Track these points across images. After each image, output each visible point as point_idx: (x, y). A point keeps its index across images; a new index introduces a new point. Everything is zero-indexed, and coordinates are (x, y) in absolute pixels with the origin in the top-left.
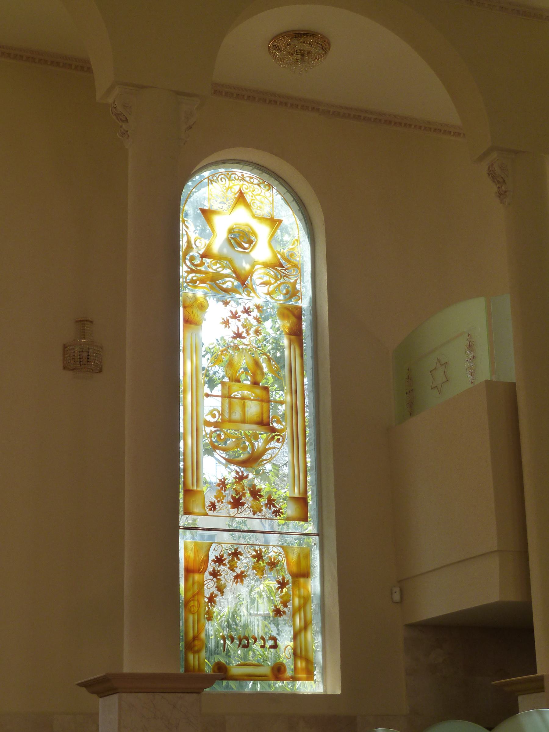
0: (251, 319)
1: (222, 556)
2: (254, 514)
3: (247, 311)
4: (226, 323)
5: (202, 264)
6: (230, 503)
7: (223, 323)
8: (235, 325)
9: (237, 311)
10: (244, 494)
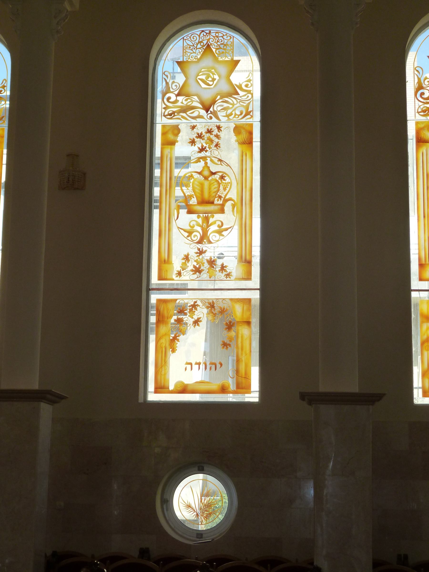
0: (212, 137)
2: (210, 278)
3: (209, 131)
6: (192, 270)
7: (190, 142)
8: (199, 143)
9: (202, 132)
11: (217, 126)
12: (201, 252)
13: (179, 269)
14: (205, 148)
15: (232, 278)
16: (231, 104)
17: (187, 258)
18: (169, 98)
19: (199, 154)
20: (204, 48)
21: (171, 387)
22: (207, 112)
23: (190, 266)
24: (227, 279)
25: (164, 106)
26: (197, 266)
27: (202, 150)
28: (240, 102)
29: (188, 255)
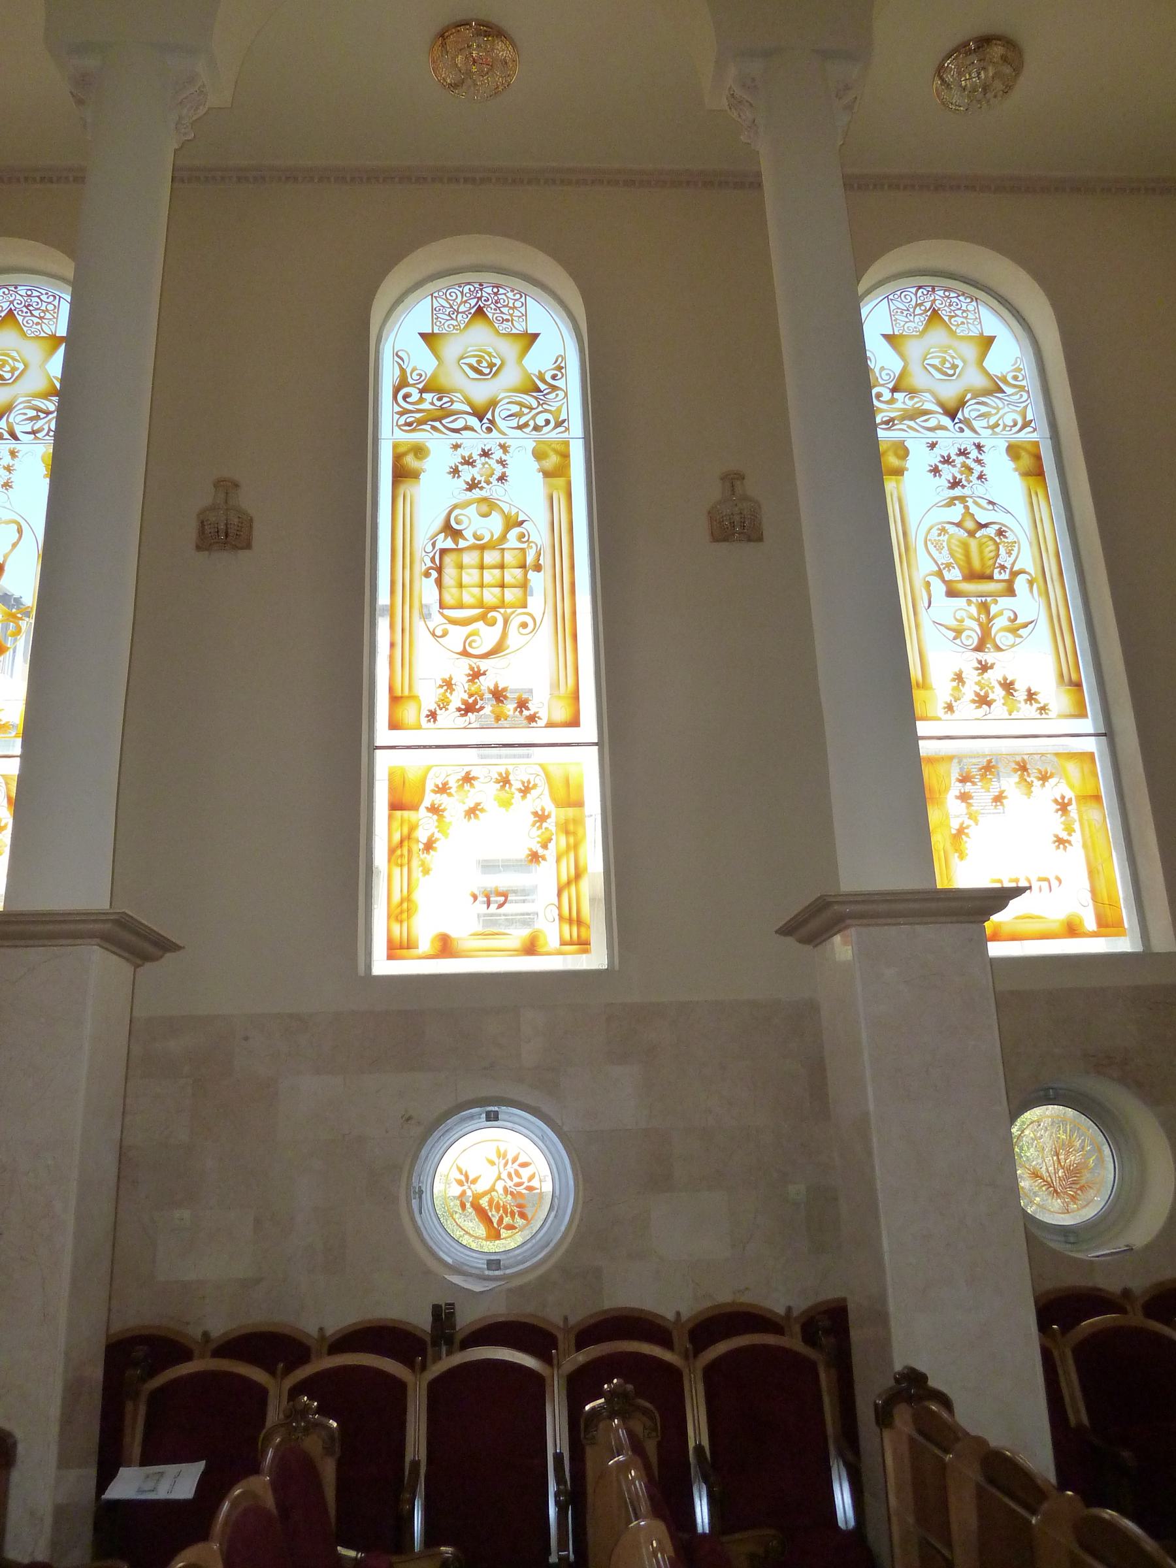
1: (445, 784)
4: (455, 472)
6: (459, 710)
7: (450, 473)
11: (500, 445)
12: (476, 675)
13: (433, 707)
14: (479, 482)
15: (541, 723)
18: (405, 397)
19: (468, 493)
20: (473, 311)
23: (457, 699)
25: (397, 409)
29: (451, 678)
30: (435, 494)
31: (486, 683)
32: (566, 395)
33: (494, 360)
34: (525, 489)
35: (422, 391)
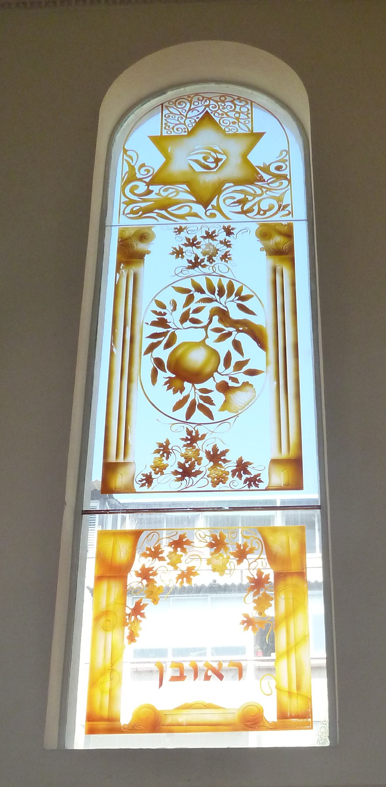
3: (210, 236)
4: (179, 253)
5: (149, 192)
6: (176, 473)
8: (190, 253)
10: (199, 461)
11: (224, 228)
12: (192, 439)
13: (148, 471)
14: (203, 260)
15: (262, 486)
16: (251, 195)
17: (165, 449)
20: (200, 116)
21: (125, 720)
22: (205, 207)
23: (173, 462)
24: (251, 488)
25: (124, 199)
26: (187, 465)
27: (195, 264)
28: (266, 191)
29: (168, 443)
30: (161, 274)
31: (203, 447)
32: (289, 181)
33: (219, 156)
34: (249, 265)
35: (148, 184)
